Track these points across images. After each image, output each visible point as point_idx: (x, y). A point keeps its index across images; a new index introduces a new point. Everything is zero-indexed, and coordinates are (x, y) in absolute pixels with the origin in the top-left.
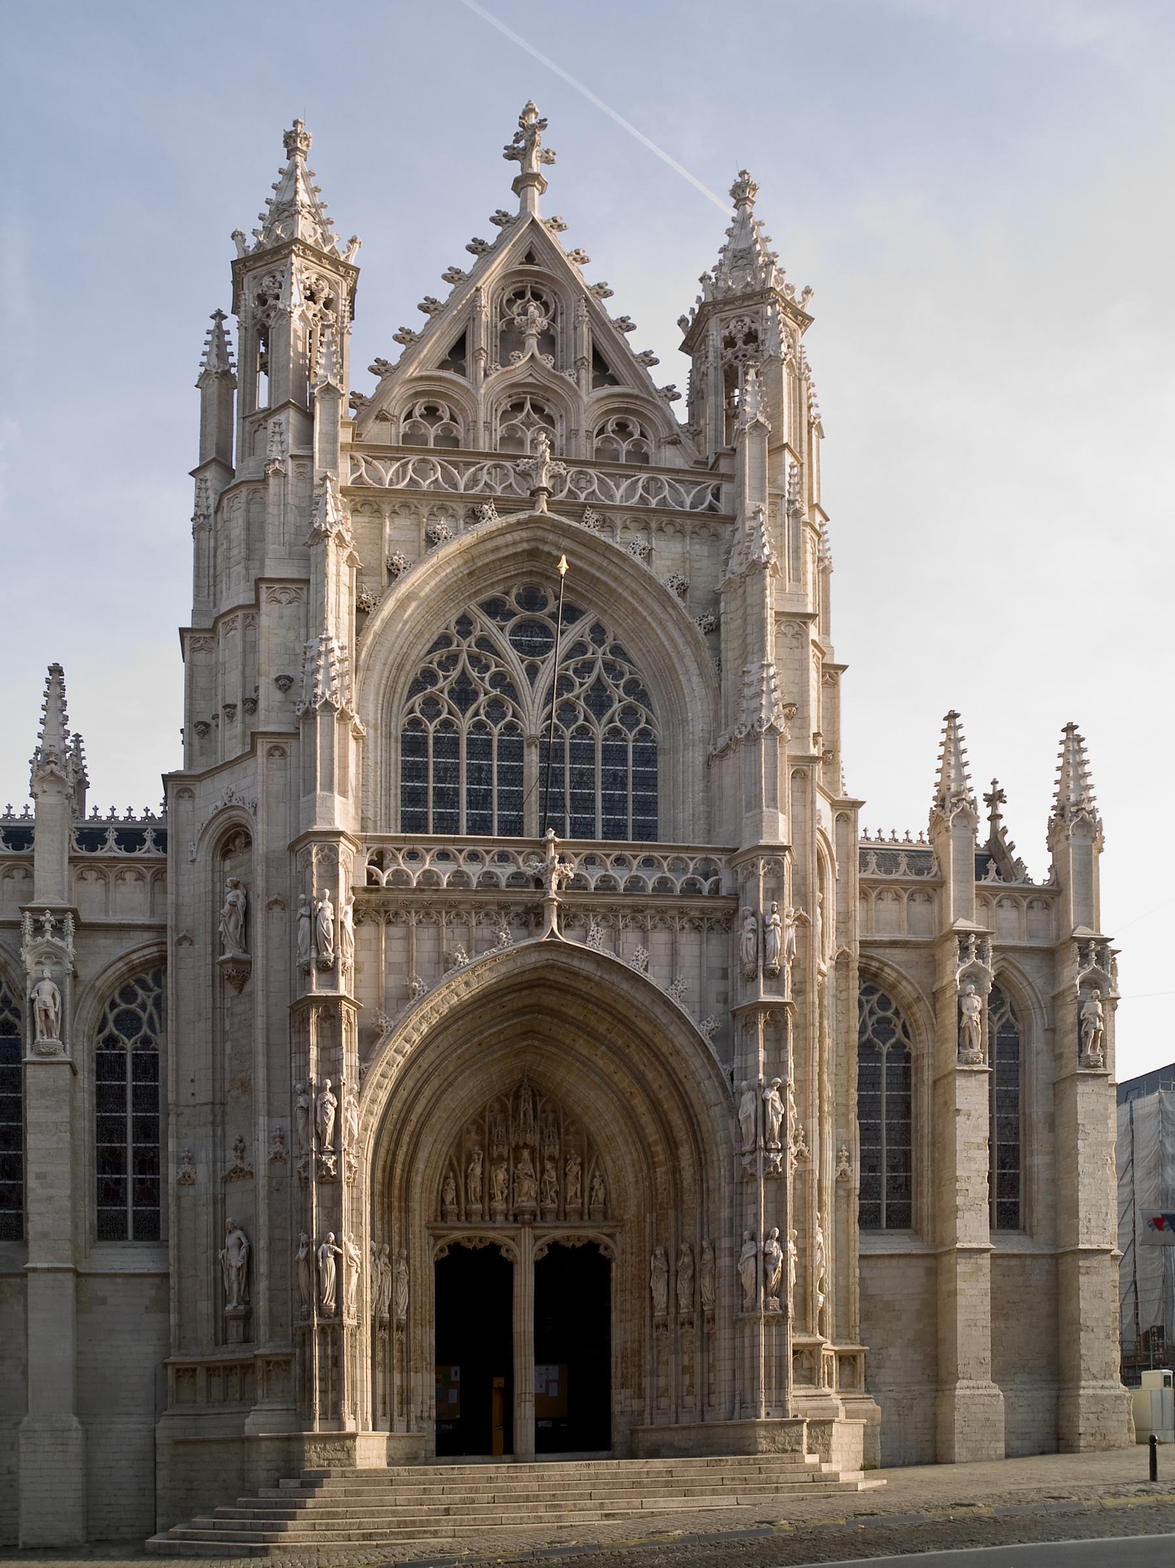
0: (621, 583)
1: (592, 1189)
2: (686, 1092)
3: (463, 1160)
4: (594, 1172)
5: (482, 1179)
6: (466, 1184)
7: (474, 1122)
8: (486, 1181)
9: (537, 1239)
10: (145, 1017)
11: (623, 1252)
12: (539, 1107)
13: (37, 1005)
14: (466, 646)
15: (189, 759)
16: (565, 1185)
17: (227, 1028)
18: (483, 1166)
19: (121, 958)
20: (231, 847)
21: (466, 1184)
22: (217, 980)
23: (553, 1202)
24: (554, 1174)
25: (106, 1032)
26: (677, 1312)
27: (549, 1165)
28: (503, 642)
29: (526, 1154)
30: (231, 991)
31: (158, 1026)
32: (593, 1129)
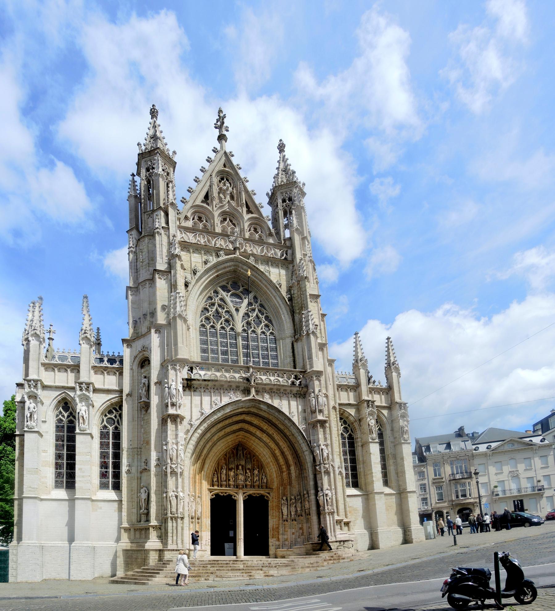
0: (262, 283)
1: (262, 479)
3: (220, 468)
5: (226, 475)
6: (221, 476)
8: (227, 475)
9: (244, 493)
10: (116, 420)
11: (273, 498)
12: (245, 453)
13: (80, 414)
14: (217, 300)
16: (253, 477)
17: (142, 424)
19: (108, 401)
20: (144, 364)
21: (221, 476)
22: (139, 408)
23: (249, 482)
24: (250, 474)
25: (103, 424)
26: (291, 516)
27: (248, 471)
28: (228, 299)
29: (240, 467)
30: (144, 412)
31: (120, 423)
32: (262, 460)
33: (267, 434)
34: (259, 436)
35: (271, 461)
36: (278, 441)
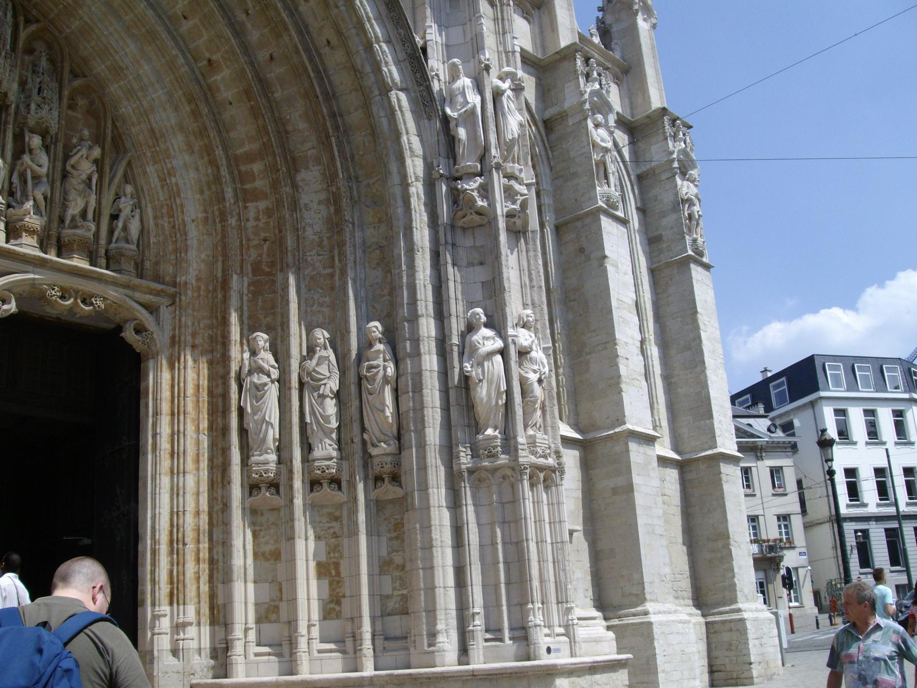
12: (23, 35)
35: (181, 128)
36: (242, 17)
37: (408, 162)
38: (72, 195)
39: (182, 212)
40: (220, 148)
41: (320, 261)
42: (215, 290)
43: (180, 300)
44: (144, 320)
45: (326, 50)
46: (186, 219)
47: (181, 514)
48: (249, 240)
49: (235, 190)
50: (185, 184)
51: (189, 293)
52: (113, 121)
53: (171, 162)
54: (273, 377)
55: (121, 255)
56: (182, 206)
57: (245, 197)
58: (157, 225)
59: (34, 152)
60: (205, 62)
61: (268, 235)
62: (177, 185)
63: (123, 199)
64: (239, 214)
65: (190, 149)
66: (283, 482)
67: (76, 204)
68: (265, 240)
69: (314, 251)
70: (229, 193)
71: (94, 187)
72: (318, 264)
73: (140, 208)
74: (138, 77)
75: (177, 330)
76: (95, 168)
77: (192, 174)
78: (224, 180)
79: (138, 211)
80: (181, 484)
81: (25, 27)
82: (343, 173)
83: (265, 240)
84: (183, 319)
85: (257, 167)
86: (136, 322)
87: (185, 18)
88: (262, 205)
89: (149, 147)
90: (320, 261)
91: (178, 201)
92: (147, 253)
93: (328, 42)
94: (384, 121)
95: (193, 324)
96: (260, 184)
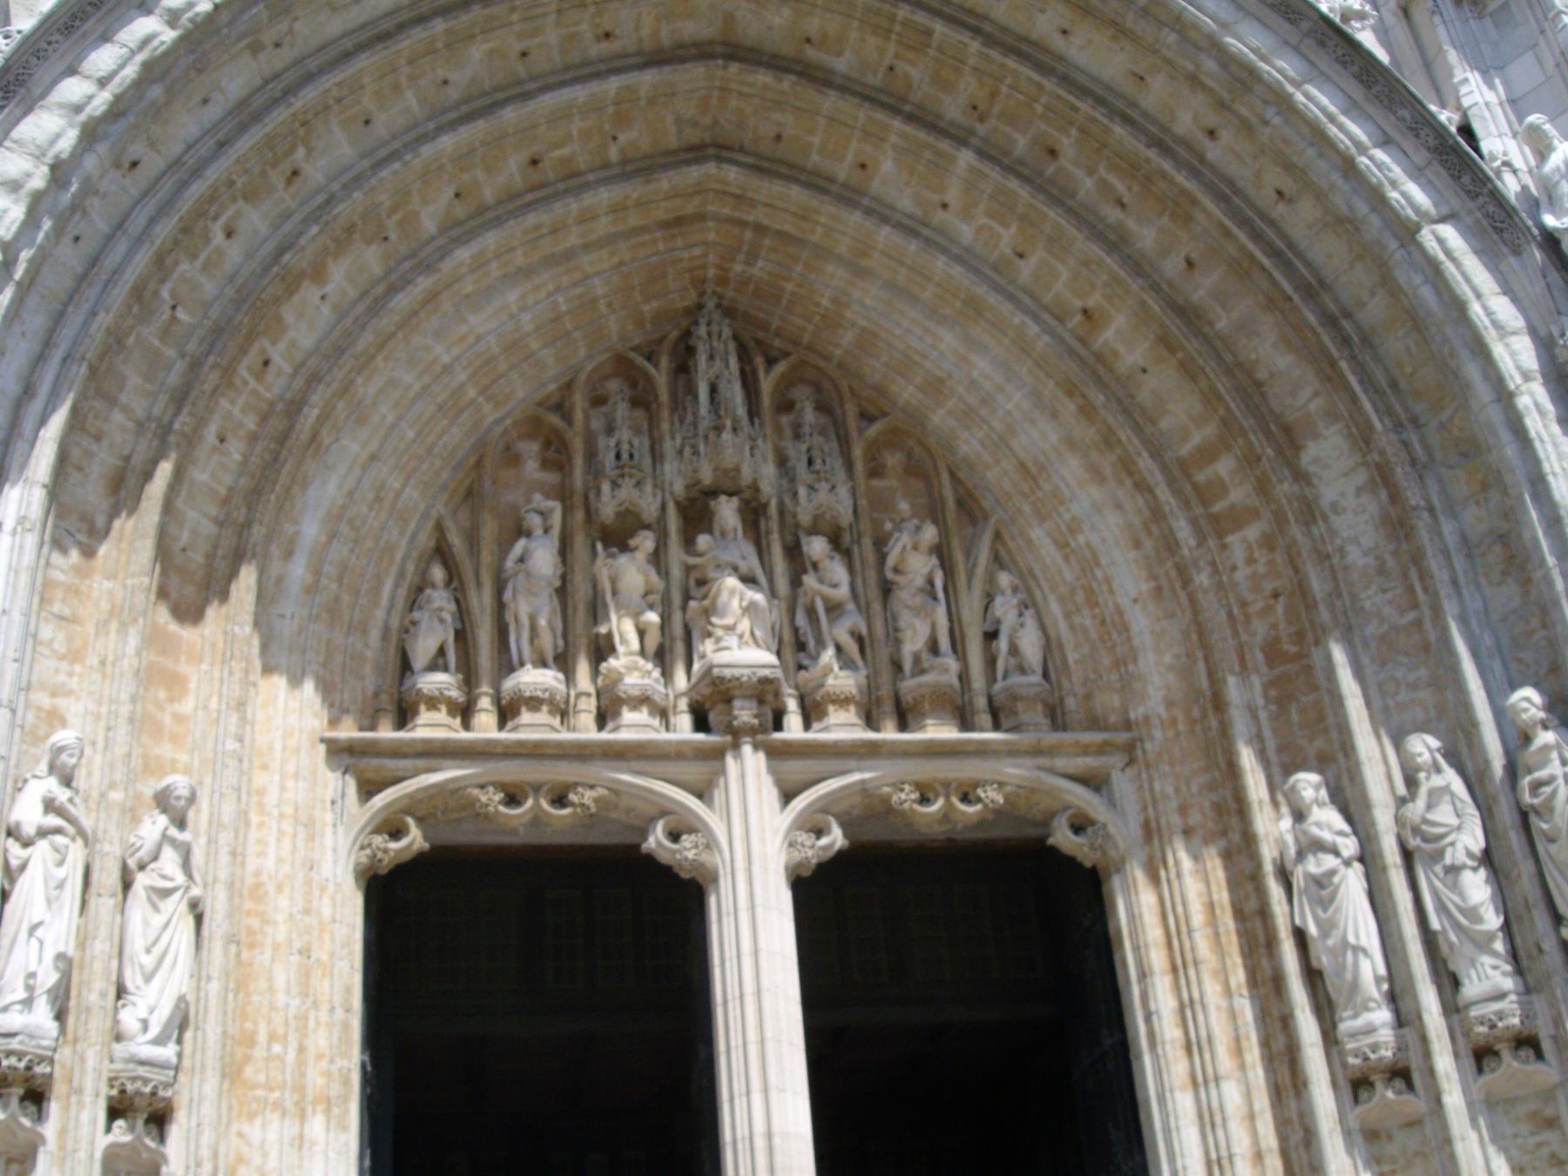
2: (1291, 246)
4: (991, 580)
6: (500, 607)
7: (533, 426)
12: (767, 384)
15: (281, 673)
18: (564, 550)
27: (817, 547)
29: (727, 511)
33: (982, 154)
34: (905, 202)
35: (1071, 443)
36: (1113, 214)
37: (1498, 350)
38: (905, 619)
39: (1111, 592)
40: (1145, 455)
41: (1390, 602)
42: (1204, 716)
43: (1144, 751)
44: (1082, 805)
45: (1281, 209)
46: (1120, 600)
47: (1225, 1162)
48: (1244, 604)
49: (1194, 523)
50: (1104, 540)
51: (1158, 734)
52: (952, 474)
53: (1068, 510)
54: (1346, 853)
55: (1015, 698)
56: (1108, 580)
57: (1218, 527)
58: (1072, 628)
59: (821, 565)
60: (1079, 318)
61: (1277, 584)
62: (1088, 545)
63: (999, 600)
64: (1213, 564)
65: (1098, 476)
66: (1415, 1064)
67: (915, 631)
68: (1276, 595)
69: (1374, 588)
70: (1183, 531)
71: (941, 595)
72: (1387, 610)
73: (1035, 605)
74: (973, 385)
75: (1150, 809)
76: (934, 561)
77: (1113, 519)
78: (1167, 509)
79: (1029, 613)
80: (1215, 1104)
81: (768, 371)
82: (1381, 421)
83: (1276, 595)
84: (1157, 786)
85: (1224, 467)
86: (1070, 812)
87: (1021, 256)
88: (1253, 532)
89: (1024, 495)
90: (1390, 602)
91: (1099, 574)
92: (1065, 683)
93: (1279, 193)
94: (1426, 292)
95: (1177, 790)
96: (1239, 494)
